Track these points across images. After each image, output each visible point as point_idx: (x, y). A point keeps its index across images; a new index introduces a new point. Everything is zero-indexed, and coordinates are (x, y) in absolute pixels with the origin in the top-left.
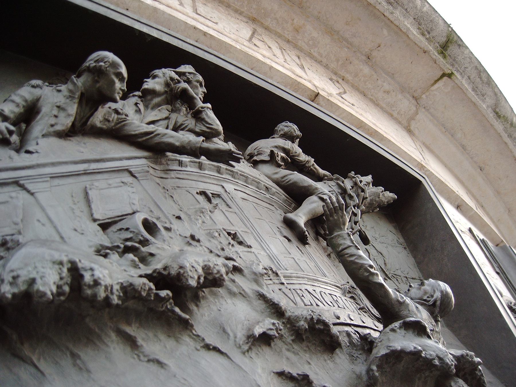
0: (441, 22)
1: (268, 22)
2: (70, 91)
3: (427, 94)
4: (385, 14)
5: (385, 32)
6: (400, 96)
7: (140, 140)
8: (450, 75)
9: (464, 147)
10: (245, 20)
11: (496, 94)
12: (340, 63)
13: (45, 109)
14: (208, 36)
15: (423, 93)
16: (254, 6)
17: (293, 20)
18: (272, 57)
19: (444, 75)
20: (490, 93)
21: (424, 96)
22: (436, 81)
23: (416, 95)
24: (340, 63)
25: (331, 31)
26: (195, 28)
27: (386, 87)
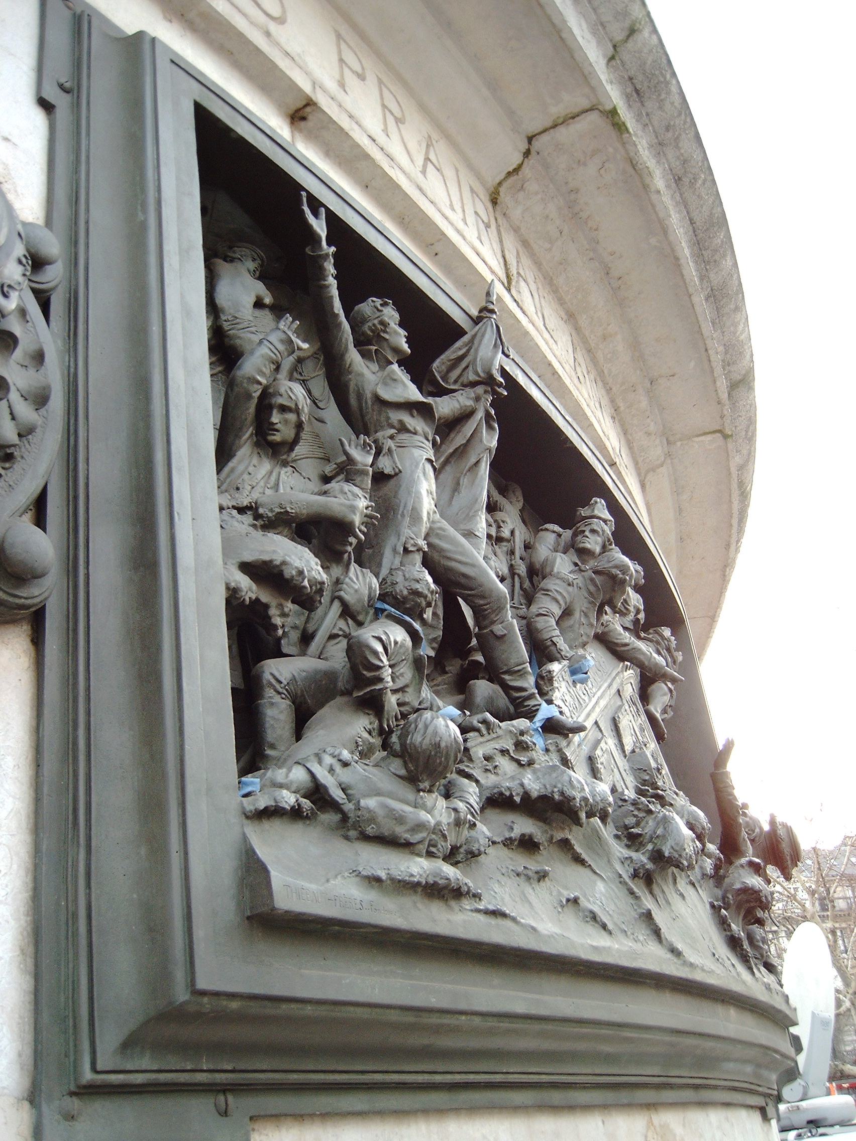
0: (748, 357)
1: (583, 321)
2: (590, 593)
3: (685, 442)
4: (710, 352)
5: (692, 364)
6: (658, 442)
7: (618, 649)
8: (726, 437)
9: (680, 510)
10: (563, 314)
11: (749, 454)
12: (623, 387)
13: (577, 614)
14: (556, 376)
15: (680, 440)
16: (580, 297)
17: (609, 325)
18: (576, 380)
19: (719, 431)
20: (745, 452)
21: (679, 444)
22: (705, 434)
23: (671, 439)
24: (623, 387)
25: (635, 345)
26: (550, 364)
27: (652, 428)
